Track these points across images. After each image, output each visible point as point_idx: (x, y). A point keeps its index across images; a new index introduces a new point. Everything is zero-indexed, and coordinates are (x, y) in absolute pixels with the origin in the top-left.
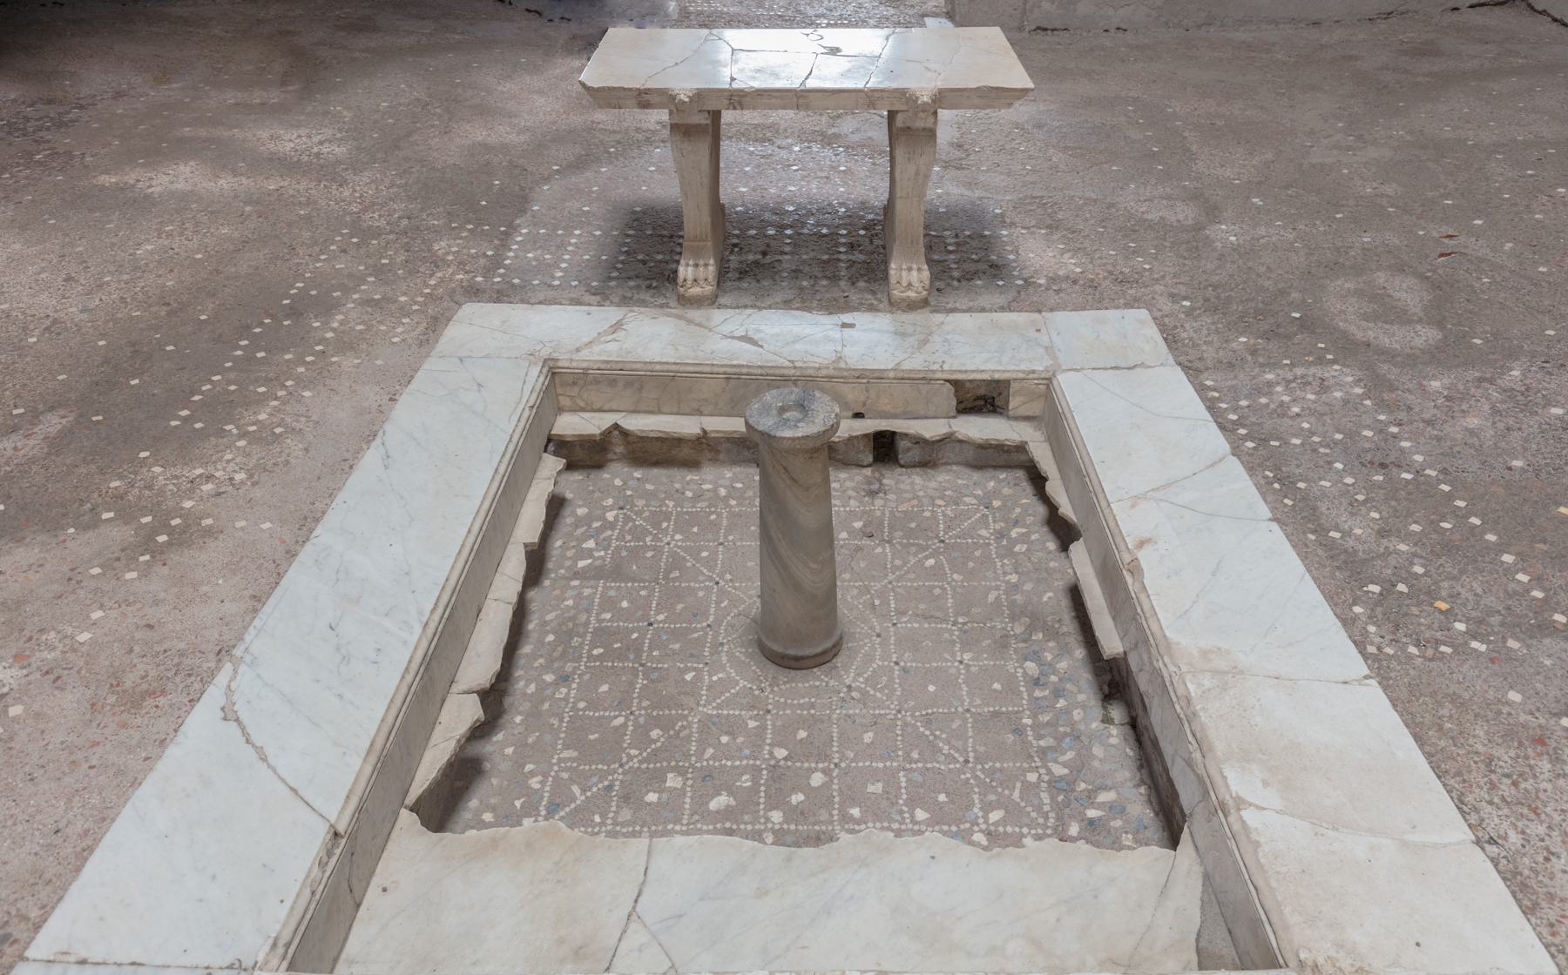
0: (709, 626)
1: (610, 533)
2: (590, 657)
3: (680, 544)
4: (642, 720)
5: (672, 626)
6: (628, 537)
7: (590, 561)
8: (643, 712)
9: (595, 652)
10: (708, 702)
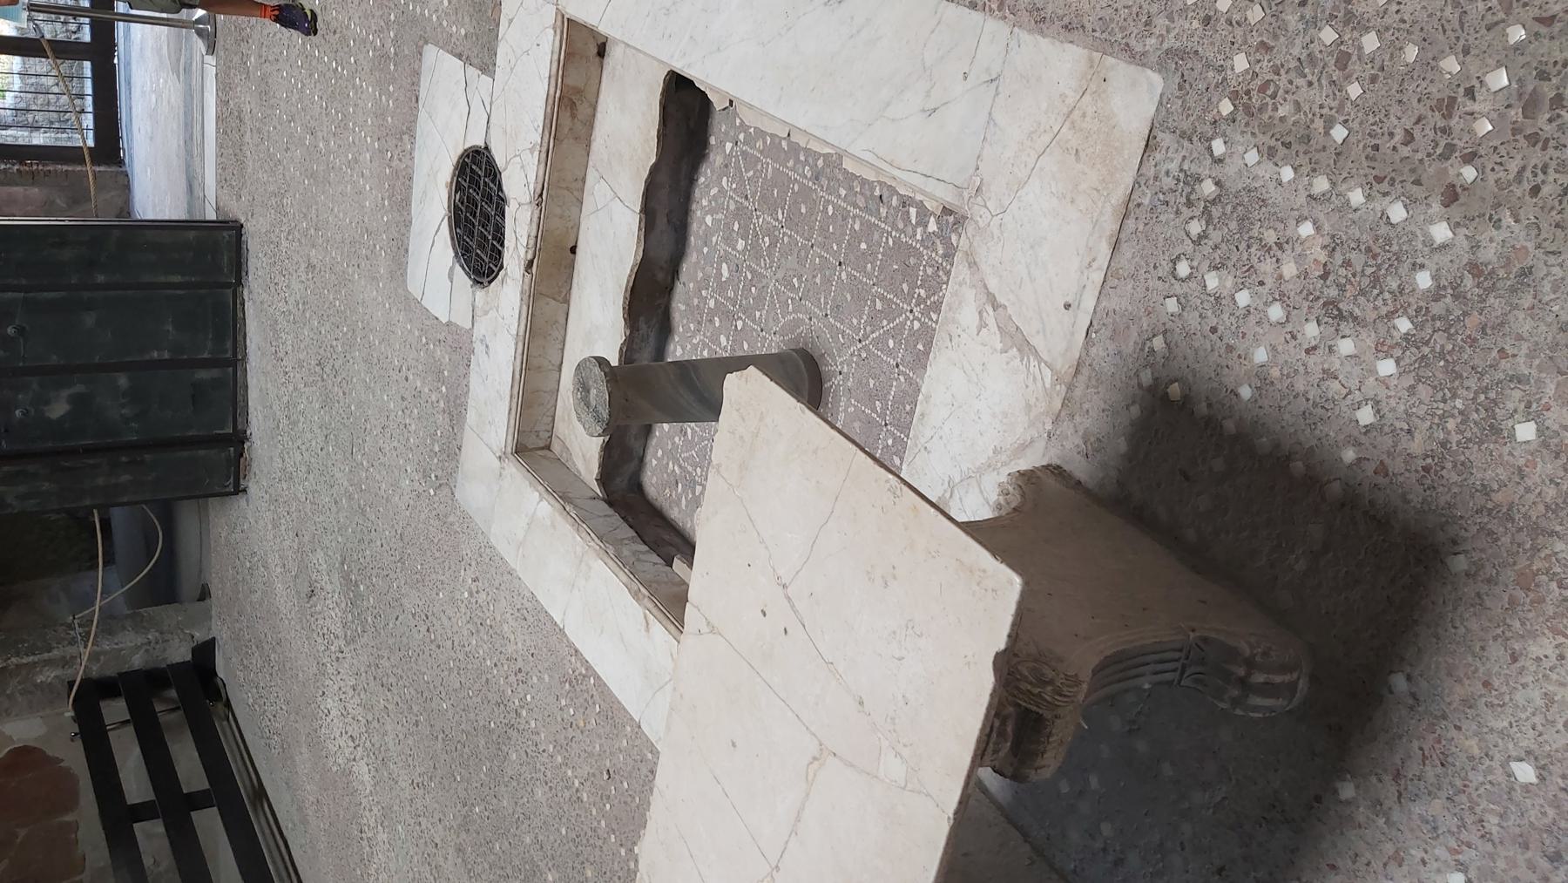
0: (827, 315)
1: (941, 252)
2: (828, 202)
3: (909, 323)
4: (777, 233)
5: (834, 283)
6: (930, 271)
7: (914, 222)
8: (781, 236)
9: (830, 208)
10: (776, 289)
